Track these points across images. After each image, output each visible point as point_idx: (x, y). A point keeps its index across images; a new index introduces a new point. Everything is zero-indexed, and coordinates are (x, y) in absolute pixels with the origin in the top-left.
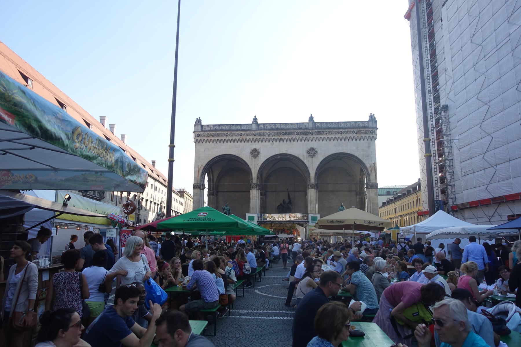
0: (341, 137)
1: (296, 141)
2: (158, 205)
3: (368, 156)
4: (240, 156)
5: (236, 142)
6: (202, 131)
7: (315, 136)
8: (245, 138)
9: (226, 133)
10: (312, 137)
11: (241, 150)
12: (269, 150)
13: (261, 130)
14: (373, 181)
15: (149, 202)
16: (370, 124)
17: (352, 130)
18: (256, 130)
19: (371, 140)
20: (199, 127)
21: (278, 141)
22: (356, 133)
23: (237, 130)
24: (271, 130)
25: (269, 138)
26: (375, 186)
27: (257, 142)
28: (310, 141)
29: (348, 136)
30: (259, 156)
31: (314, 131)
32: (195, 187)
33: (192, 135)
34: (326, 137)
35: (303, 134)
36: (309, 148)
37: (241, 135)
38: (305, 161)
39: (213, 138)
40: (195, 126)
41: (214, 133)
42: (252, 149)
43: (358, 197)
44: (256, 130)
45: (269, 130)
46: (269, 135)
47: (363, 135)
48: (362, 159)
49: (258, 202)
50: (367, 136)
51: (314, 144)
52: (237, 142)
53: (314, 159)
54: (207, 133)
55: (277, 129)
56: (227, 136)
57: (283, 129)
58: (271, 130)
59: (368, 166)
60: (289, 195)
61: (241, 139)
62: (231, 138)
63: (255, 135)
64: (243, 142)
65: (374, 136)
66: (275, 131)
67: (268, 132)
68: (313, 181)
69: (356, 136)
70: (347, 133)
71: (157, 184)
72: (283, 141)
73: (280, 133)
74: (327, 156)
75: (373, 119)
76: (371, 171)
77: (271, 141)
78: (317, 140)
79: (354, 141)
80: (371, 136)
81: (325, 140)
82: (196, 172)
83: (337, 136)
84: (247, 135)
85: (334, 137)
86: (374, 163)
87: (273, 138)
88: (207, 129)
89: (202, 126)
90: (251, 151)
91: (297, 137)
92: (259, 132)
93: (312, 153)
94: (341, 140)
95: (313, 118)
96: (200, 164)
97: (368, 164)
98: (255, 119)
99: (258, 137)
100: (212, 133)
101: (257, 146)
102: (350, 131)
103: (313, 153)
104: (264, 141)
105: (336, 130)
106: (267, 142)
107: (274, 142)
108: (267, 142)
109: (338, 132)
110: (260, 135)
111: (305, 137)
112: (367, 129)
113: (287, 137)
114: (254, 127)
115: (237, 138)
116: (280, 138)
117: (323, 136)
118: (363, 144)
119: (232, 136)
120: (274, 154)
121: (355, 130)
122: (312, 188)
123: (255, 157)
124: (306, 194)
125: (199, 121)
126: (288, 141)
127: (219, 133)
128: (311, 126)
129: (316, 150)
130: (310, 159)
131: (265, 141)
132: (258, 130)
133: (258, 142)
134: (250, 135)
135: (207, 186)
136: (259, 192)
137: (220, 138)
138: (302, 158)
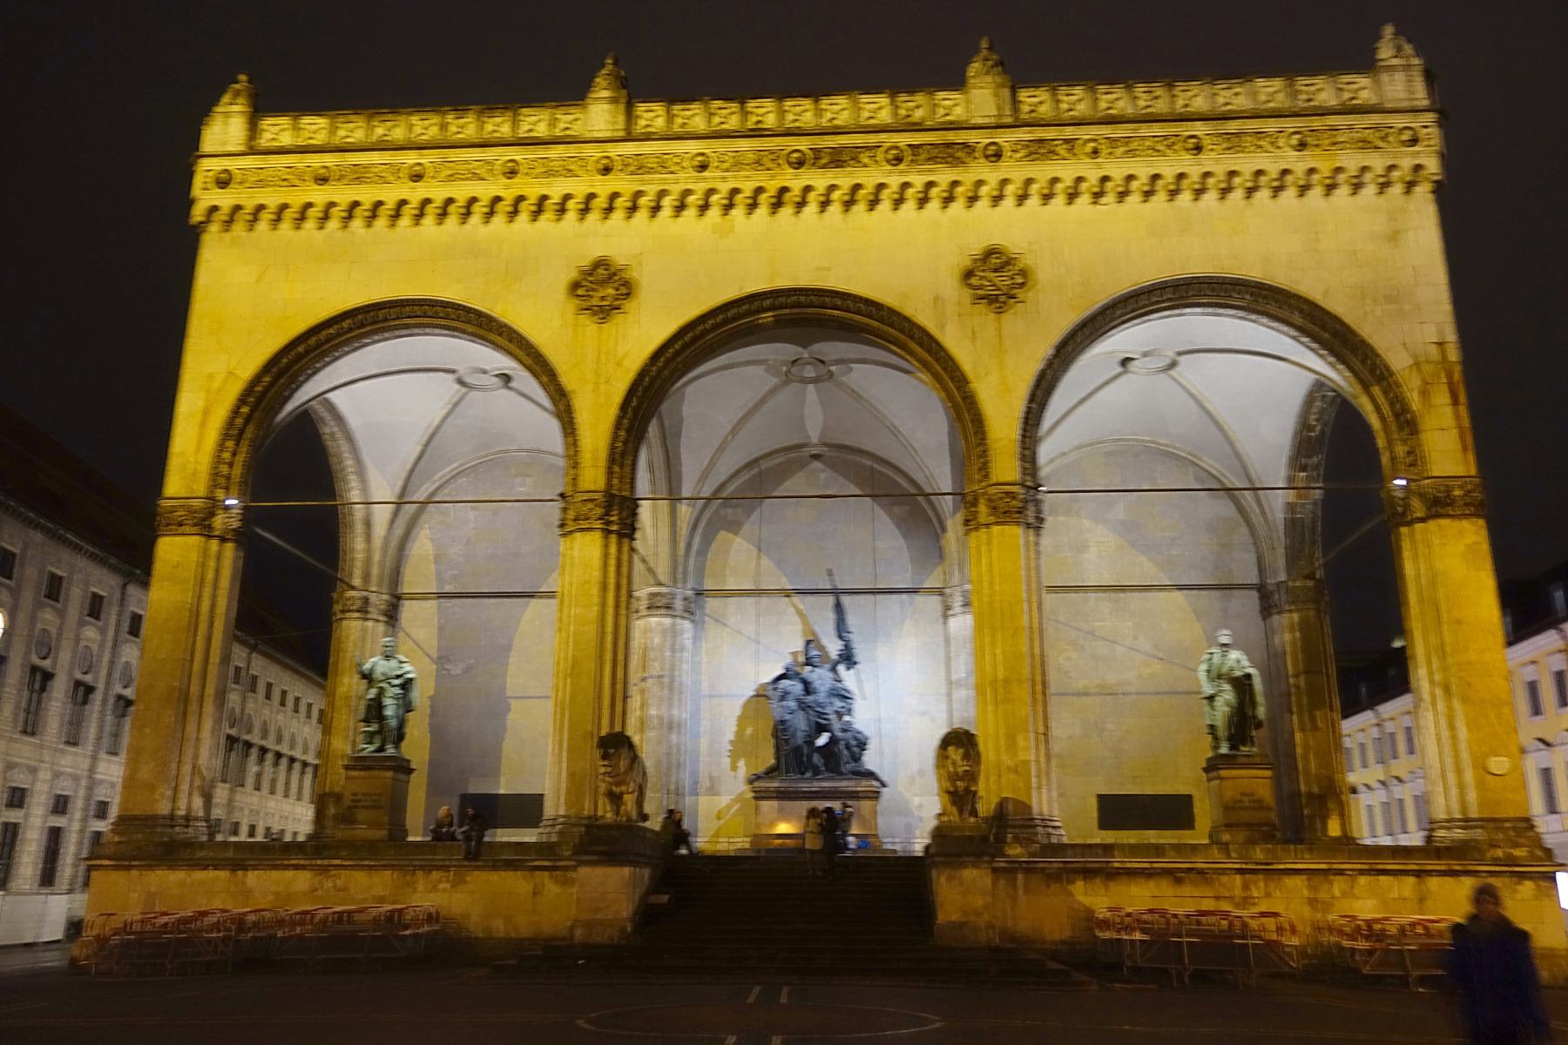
0: (1195, 172)
3: (1390, 299)
7: (1015, 170)
9: (410, 158)
10: (991, 175)
13: (647, 137)
15: (59, 689)
17: (1270, 126)
22: (1302, 146)
25: (700, 188)
29: (1246, 164)
30: (629, 305)
31: (1005, 138)
34: (1093, 176)
35: (932, 159)
36: (977, 248)
39: (319, 196)
41: (330, 160)
42: (586, 262)
46: (703, 167)
47: (1351, 161)
48: (1348, 320)
50: (1378, 163)
53: (1012, 321)
56: (417, 178)
59: (1397, 361)
61: (509, 195)
63: (607, 170)
66: (744, 144)
67: (693, 147)
69: (1299, 164)
70: (1233, 142)
76: (1425, 394)
80: (1406, 163)
83: (1168, 168)
84: (550, 173)
85: (1143, 170)
87: (724, 188)
91: (894, 181)
92: (630, 148)
93: (996, 280)
99: (624, 184)
100: (316, 161)
102: (1259, 134)
103: (1002, 280)
104: (667, 211)
105: (1157, 129)
106: (690, 213)
109: (1170, 142)
110: (640, 167)
111: (943, 176)
112: (1375, 119)
113: (820, 180)
116: (772, 186)
117: (1067, 171)
119: (451, 178)
121: (1290, 124)
123: (604, 313)
129: (1027, 261)
130: (984, 317)
132: (629, 138)
134: (570, 173)
137: (366, 195)
138: (925, 319)
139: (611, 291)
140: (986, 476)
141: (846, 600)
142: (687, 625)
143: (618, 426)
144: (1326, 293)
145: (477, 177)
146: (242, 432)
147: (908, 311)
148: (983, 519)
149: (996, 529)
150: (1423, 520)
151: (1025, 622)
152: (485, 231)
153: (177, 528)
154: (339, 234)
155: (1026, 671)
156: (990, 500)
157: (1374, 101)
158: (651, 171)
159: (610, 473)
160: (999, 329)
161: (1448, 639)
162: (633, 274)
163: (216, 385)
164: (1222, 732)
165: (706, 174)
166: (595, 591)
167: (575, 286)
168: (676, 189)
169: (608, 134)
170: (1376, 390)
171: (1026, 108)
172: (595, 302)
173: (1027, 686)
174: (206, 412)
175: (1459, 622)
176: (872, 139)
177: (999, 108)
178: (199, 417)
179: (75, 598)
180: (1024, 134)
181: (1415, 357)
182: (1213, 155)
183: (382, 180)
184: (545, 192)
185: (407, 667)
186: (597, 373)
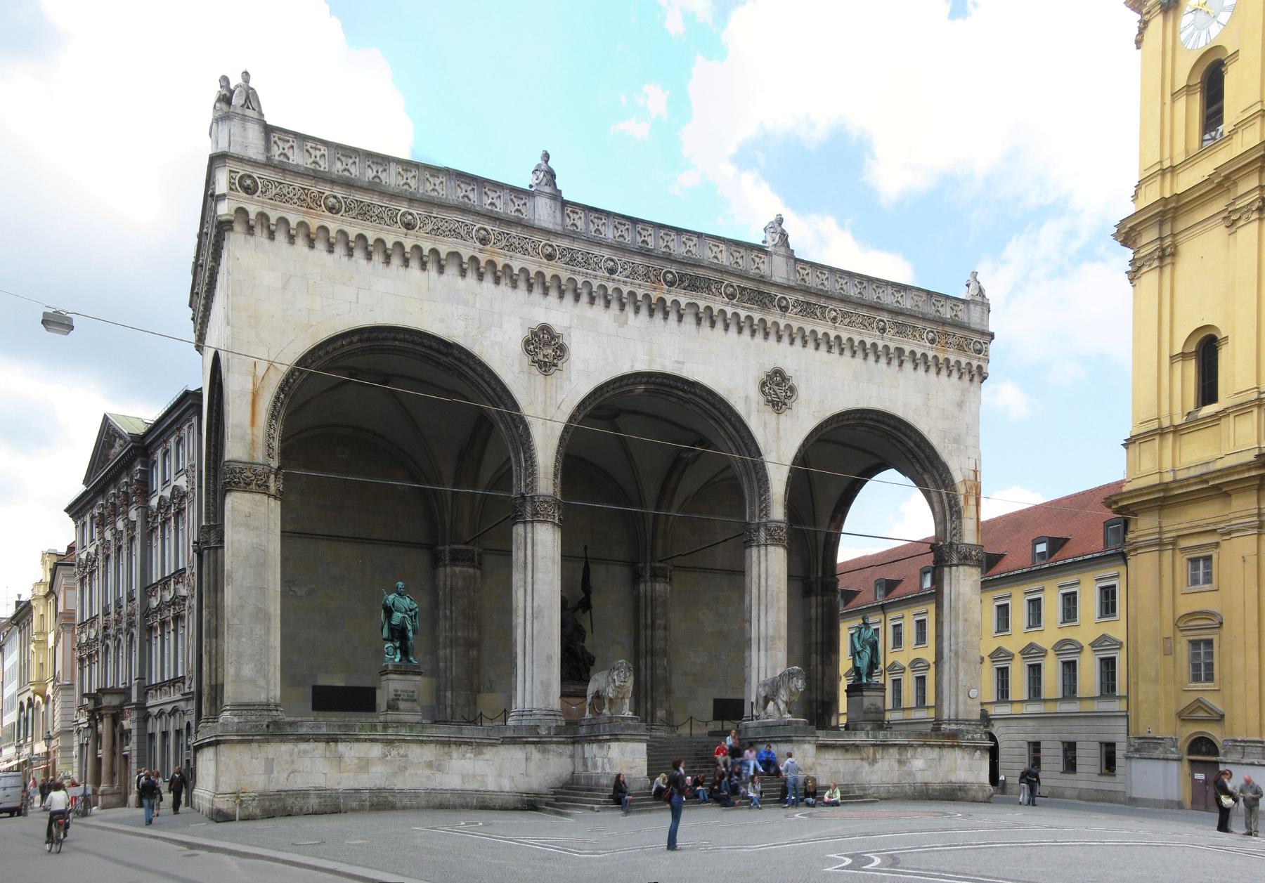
4: (476, 350)
21: (644, 311)
24: (620, 248)
42: (535, 326)
45: (610, 246)
46: (612, 271)
55: (645, 253)
57: (668, 258)
58: (620, 248)
63: (550, 257)
66: (638, 260)
67: (607, 253)
87: (626, 290)
116: (655, 296)
122: (777, 542)
131: (592, 301)
132: (564, 235)
148: (762, 541)
149: (771, 548)
153: (246, 487)
156: (767, 529)
165: (615, 276)
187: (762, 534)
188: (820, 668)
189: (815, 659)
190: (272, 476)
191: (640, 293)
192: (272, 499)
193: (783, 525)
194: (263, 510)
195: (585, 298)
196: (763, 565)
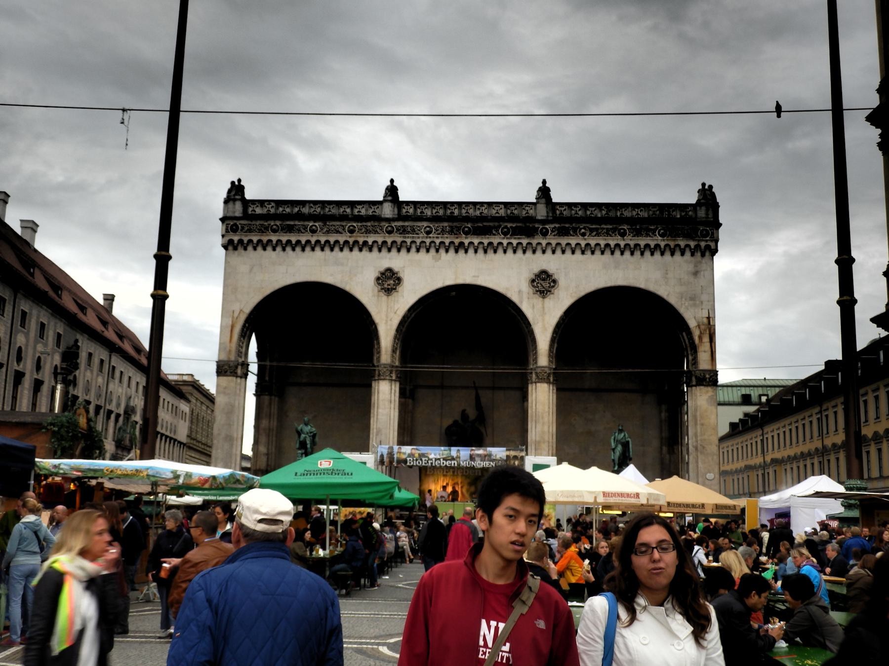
0: (622, 244)
1: (500, 251)
2: (118, 416)
3: (693, 298)
4: (347, 288)
5: (337, 249)
6: (246, 216)
8: (361, 240)
10: (544, 242)
11: (354, 272)
12: (428, 272)
14: (704, 363)
16: (702, 213)
18: (393, 220)
19: (703, 255)
20: (237, 209)
21: (452, 251)
23: (343, 218)
24: (435, 219)
25: (428, 241)
26: (710, 379)
27: (394, 251)
28: (539, 252)
30: (400, 289)
32: (223, 369)
33: (219, 227)
34: (583, 243)
36: (536, 270)
37: (351, 232)
38: (525, 308)
39: (274, 238)
40: (226, 202)
41: (278, 223)
42: (382, 269)
43: (664, 407)
44: (393, 220)
46: (428, 233)
47: (682, 243)
49: (395, 414)
51: (550, 262)
52: (341, 250)
53: (549, 302)
54: (258, 223)
55: (451, 218)
56: (313, 232)
57: (467, 219)
58: (435, 219)
59: (692, 324)
60: (478, 398)
61: (351, 240)
62: (323, 239)
63: (390, 232)
64: (356, 250)
65: (712, 245)
67: (425, 224)
68: (543, 359)
70: (638, 233)
71: (116, 361)
72: (466, 251)
73: (458, 229)
74: (583, 294)
75: (708, 197)
76: (700, 338)
77: (433, 251)
78: (559, 251)
79: (657, 255)
80: (703, 244)
81: (578, 252)
82: (227, 329)
84: (368, 232)
85: (603, 243)
86: (709, 318)
87: (438, 241)
88: (259, 211)
89: (246, 203)
90: (377, 274)
91: (505, 242)
94: (622, 253)
95: (548, 190)
96: (236, 307)
97: (692, 317)
98: (392, 190)
101: (395, 261)
104: (413, 249)
106: (423, 251)
107: (442, 251)
108: (423, 251)
109: (614, 230)
110: (403, 231)
111: (525, 242)
113: (476, 241)
114: (388, 211)
115: (342, 239)
116: (457, 241)
117: (573, 241)
118: (681, 264)
119: (328, 232)
120: (439, 284)
122: (540, 380)
123: (389, 291)
124: (525, 397)
125: (237, 189)
126: (481, 251)
127: (292, 223)
128: (541, 212)
129: (555, 277)
130: (537, 300)
131: (418, 250)
132: (400, 217)
133: (399, 250)
134: (376, 232)
135: (254, 368)
136: (396, 387)
138: (515, 298)
139: (392, 282)
140: (536, 363)
141: (480, 392)
142: (410, 401)
143: (395, 337)
144: (668, 295)
145: (338, 232)
146: (245, 334)
147: (509, 295)
149: (538, 385)
150: (695, 386)
151: (546, 419)
152: (340, 254)
154: (282, 253)
155: (546, 438)
157: (694, 216)
158: (408, 233)
159: (393, 356)
160: (543, 304)
161: (699, 431)
162: (401, 275)
163: (236, 315)
164: (617, 461)
166: (387, 403)
167: (378, 279)
168: (418, 241)
169: (391, 216)
170: (684, 334)
171: (558, 212)
172: (386, 286)
173: (546, 444)
174: (232, 327)
175: (702, 425)
176: (496, 224)
177: (547, 213)
178: (229, 329)
179: (96, 361)
180: (557, 226)
181: (698, 323)
182: (630, 237)
183: (299, 231)
184: (366, 239)
185: (314, 429)
186: (387, 317)
187: (534, 376)
188: (668, 456)
189: (665, 449)
190: (240, 367)
191: (447, 242)
192: (239, 379)
193: (546, 369)
194: (232, 384)
195: (413, 249)
196: (534, 396)
